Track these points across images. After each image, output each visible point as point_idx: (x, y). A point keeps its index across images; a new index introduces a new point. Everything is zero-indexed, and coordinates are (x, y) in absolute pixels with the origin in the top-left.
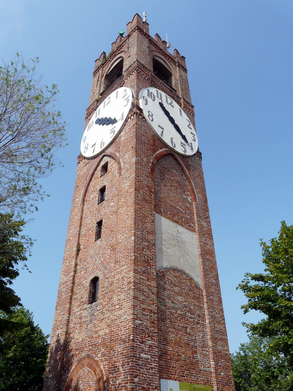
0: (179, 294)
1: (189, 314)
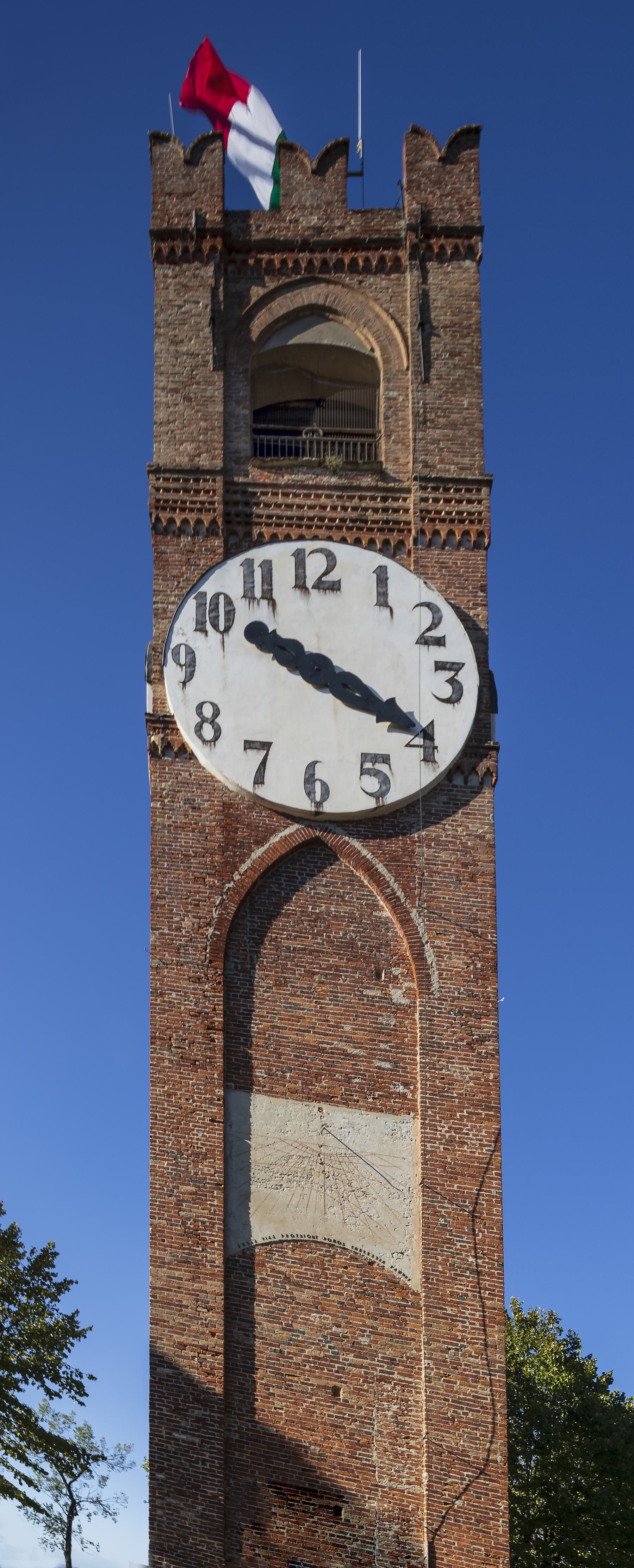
0: (317, 1306)
1: (351, 1357)
